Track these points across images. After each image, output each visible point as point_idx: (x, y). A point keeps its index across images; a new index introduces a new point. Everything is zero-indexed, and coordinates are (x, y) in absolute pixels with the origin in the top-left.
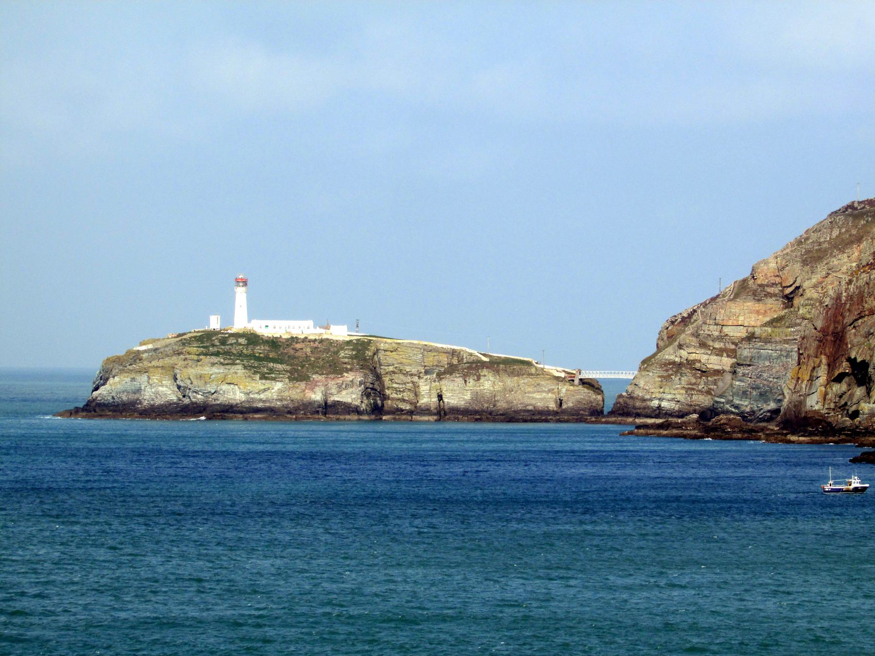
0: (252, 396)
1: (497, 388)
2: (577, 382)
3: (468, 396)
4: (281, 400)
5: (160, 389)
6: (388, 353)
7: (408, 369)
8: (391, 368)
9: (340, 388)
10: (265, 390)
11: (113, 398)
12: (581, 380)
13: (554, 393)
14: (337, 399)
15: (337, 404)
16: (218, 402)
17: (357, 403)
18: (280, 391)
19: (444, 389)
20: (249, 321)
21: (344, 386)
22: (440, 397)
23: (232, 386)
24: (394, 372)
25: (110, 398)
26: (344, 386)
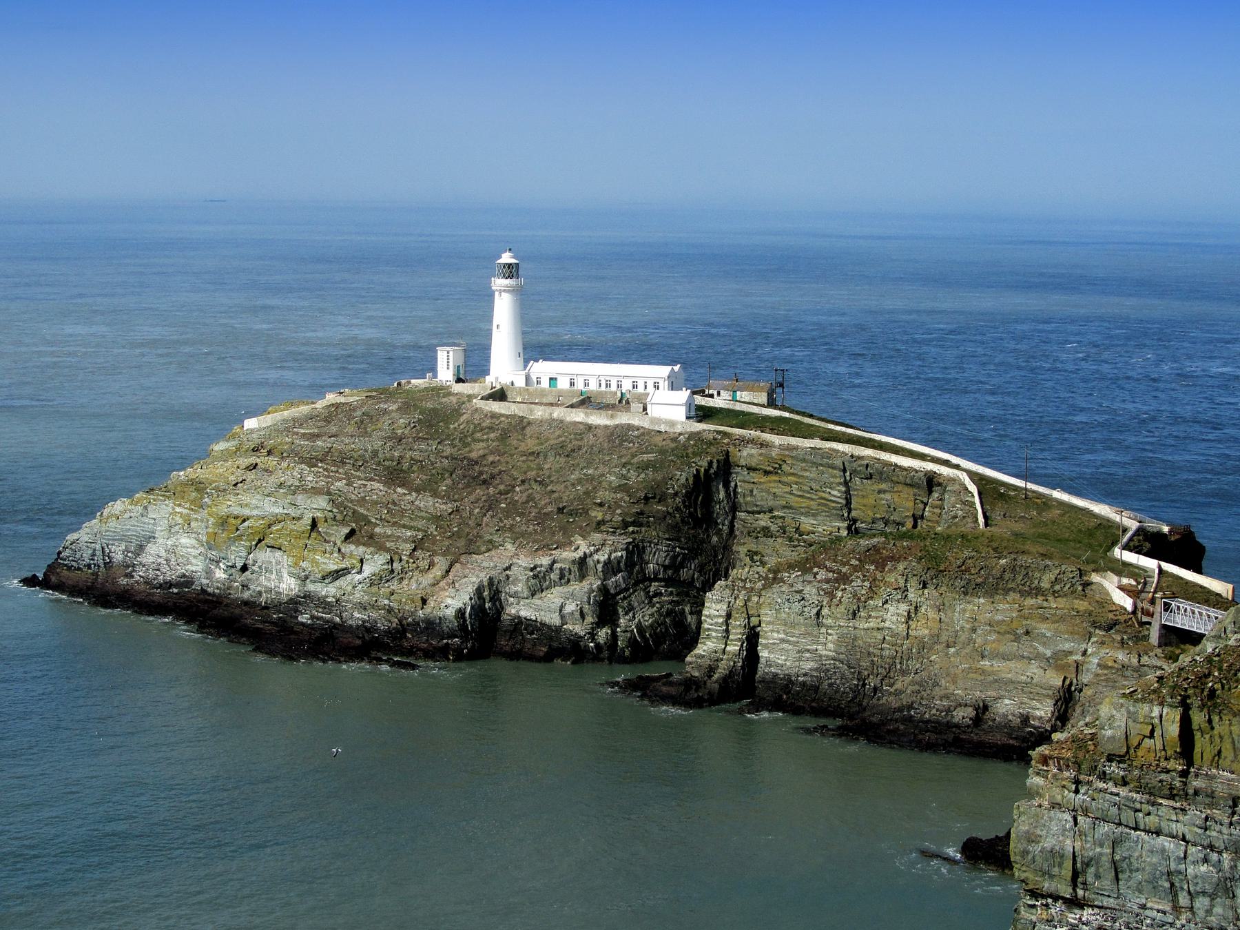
0: (311, 587)
1: (921, 630)
2: (1154, 634)
3: (828, 647)
4: (363, 607)
5: (184, 540)
6: (756, 477)
7: (807, 523)
8: (763, 521)
9: (540, 582)
10: (337, 575)
11: (93, 555)
12: (1164, 627)
13: (1059, 668)
14: (523, 613)
15: (519, 624)
16: (246, 595)
17: (578, 628)
18: (376, 581)
19: (767, 615)
20: (525, 367)
21: (554, 576)
22: (752, 638)
23: (278, 554)
24: (766, 532)
25: (86, 555)
26: (554, 576)
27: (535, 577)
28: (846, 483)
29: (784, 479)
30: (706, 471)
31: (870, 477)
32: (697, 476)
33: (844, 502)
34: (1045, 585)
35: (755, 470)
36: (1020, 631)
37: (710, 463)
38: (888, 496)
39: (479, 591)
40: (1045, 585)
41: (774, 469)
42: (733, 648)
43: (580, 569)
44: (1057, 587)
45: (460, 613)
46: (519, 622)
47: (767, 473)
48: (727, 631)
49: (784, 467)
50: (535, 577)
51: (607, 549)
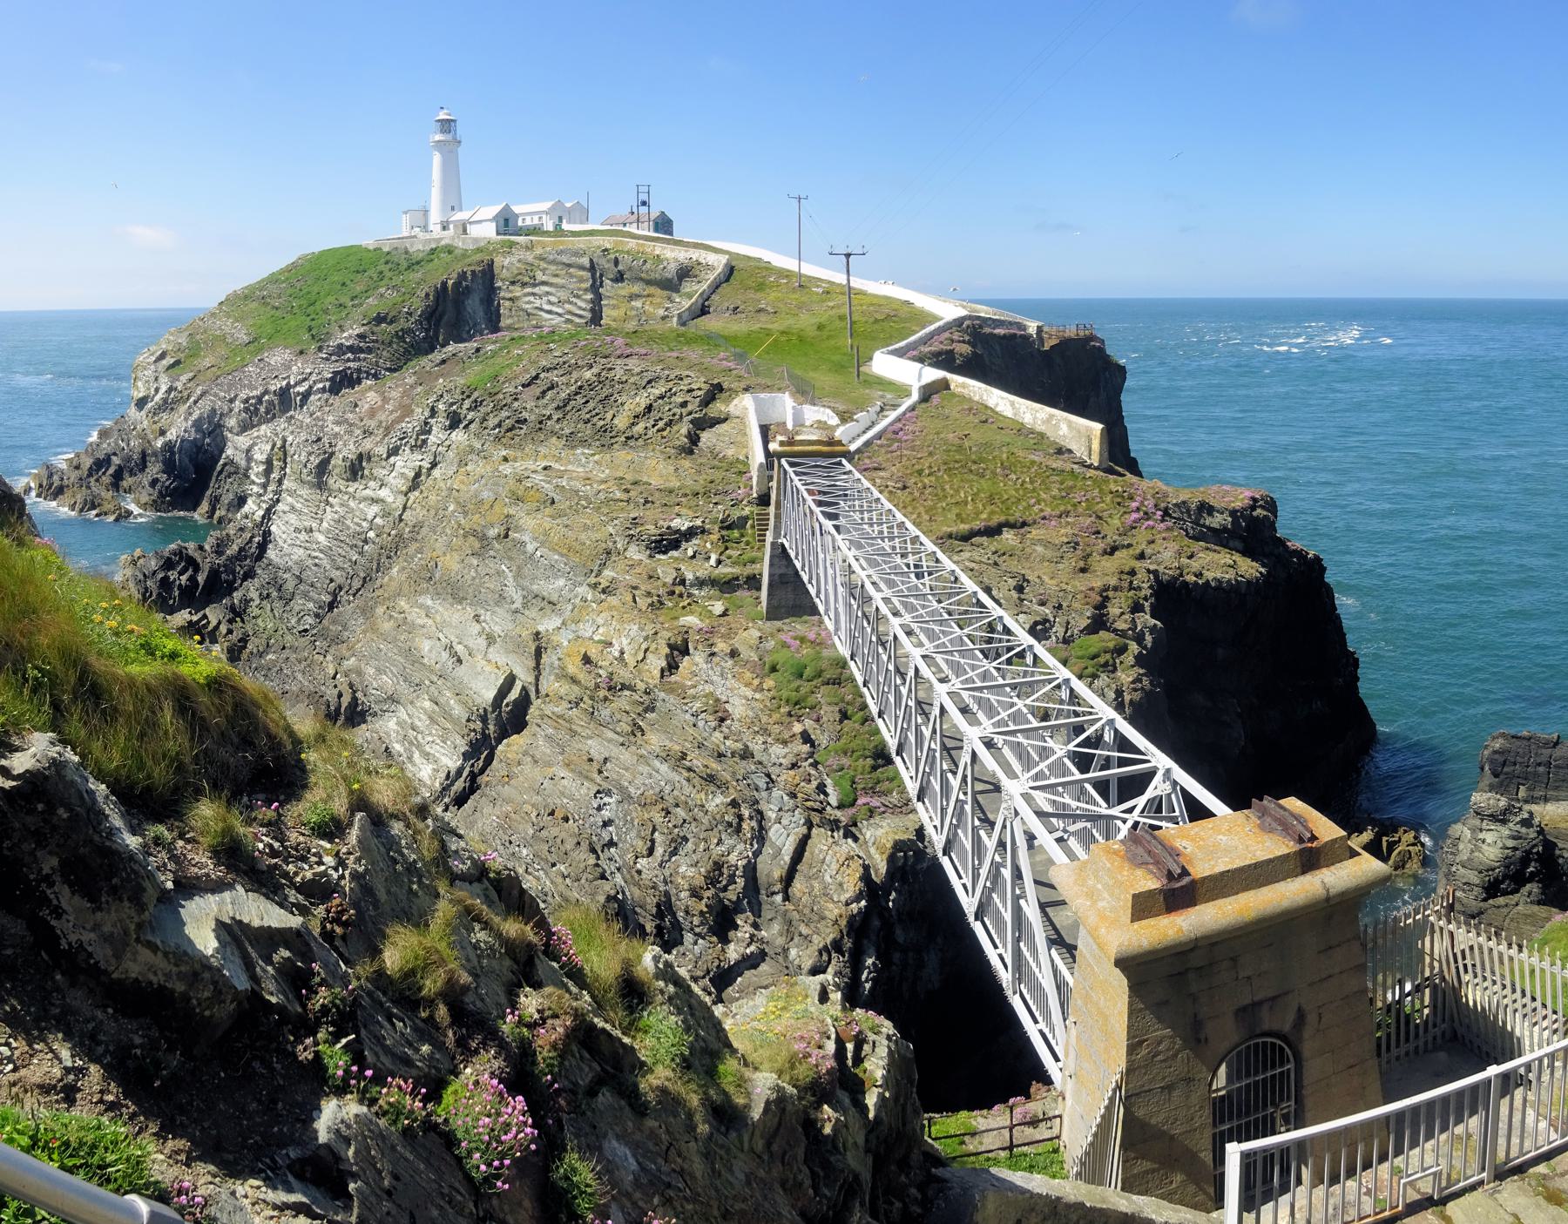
6: (517, 291)
27: (246, 410)
28: (595, 288)
29: (536, 290)
30: (457, 284)
31: (619, 278)
32: (442, 291)
33: (588, 315)
34: (621, 422)
35: (513, 283)
36: (492, 533)
37: (463, 276)
38: (637, 304)
39: (197, 424)
40: (621, 422)
41: (525, 279)
42: (261, 513)
43: (281, 403)
44: (639, 428)
45: (169, 446)
46: (231, 462)
47: (524, 285)
48: (264, 486)
49: (540, 276)
50: (246, 410)
51: (314, 377)
